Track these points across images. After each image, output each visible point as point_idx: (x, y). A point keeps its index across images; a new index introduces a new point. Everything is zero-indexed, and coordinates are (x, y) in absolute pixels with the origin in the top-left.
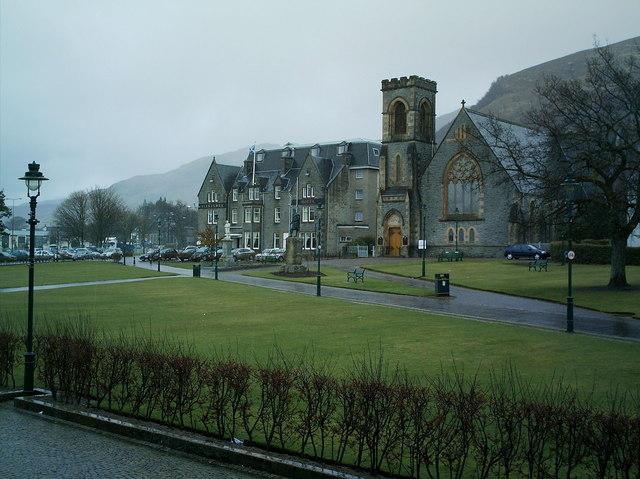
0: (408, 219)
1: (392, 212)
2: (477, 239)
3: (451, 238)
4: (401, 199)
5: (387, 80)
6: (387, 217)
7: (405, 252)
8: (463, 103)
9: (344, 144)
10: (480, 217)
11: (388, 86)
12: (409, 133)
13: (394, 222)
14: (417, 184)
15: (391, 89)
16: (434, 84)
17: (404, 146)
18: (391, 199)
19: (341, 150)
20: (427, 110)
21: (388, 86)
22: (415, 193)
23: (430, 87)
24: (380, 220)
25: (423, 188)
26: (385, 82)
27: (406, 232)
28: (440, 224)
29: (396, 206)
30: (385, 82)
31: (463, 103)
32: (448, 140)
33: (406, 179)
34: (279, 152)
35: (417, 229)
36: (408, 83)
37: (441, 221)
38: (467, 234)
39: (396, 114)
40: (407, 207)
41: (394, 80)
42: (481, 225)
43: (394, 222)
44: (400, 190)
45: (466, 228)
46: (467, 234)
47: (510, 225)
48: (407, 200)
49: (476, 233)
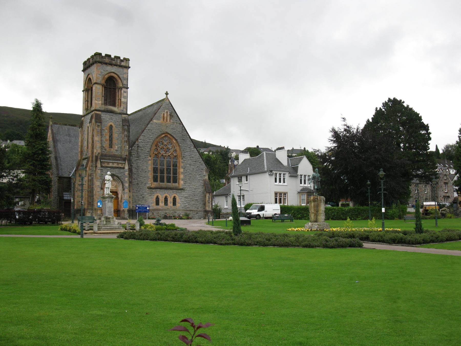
0: (127, 185)
2: (178, 205)
3: (157, 203)
4: (120, 166)
5: (100, 54)
7: (126, 215)
8: (167, 94)
10: (181, 187)
14: (130, 154)
15: (106, 64)
18: (111, 165)
25: (133, 159)
27: (126, 197)
31: (167, 94)
36: (123, 64)
37: (151, 188)
38: (170, 200)
40: (127, 173)
41: (108, 56)
46: (170, 200)
47: (207, 195)
48: (127, 167)
49: (178, 200)
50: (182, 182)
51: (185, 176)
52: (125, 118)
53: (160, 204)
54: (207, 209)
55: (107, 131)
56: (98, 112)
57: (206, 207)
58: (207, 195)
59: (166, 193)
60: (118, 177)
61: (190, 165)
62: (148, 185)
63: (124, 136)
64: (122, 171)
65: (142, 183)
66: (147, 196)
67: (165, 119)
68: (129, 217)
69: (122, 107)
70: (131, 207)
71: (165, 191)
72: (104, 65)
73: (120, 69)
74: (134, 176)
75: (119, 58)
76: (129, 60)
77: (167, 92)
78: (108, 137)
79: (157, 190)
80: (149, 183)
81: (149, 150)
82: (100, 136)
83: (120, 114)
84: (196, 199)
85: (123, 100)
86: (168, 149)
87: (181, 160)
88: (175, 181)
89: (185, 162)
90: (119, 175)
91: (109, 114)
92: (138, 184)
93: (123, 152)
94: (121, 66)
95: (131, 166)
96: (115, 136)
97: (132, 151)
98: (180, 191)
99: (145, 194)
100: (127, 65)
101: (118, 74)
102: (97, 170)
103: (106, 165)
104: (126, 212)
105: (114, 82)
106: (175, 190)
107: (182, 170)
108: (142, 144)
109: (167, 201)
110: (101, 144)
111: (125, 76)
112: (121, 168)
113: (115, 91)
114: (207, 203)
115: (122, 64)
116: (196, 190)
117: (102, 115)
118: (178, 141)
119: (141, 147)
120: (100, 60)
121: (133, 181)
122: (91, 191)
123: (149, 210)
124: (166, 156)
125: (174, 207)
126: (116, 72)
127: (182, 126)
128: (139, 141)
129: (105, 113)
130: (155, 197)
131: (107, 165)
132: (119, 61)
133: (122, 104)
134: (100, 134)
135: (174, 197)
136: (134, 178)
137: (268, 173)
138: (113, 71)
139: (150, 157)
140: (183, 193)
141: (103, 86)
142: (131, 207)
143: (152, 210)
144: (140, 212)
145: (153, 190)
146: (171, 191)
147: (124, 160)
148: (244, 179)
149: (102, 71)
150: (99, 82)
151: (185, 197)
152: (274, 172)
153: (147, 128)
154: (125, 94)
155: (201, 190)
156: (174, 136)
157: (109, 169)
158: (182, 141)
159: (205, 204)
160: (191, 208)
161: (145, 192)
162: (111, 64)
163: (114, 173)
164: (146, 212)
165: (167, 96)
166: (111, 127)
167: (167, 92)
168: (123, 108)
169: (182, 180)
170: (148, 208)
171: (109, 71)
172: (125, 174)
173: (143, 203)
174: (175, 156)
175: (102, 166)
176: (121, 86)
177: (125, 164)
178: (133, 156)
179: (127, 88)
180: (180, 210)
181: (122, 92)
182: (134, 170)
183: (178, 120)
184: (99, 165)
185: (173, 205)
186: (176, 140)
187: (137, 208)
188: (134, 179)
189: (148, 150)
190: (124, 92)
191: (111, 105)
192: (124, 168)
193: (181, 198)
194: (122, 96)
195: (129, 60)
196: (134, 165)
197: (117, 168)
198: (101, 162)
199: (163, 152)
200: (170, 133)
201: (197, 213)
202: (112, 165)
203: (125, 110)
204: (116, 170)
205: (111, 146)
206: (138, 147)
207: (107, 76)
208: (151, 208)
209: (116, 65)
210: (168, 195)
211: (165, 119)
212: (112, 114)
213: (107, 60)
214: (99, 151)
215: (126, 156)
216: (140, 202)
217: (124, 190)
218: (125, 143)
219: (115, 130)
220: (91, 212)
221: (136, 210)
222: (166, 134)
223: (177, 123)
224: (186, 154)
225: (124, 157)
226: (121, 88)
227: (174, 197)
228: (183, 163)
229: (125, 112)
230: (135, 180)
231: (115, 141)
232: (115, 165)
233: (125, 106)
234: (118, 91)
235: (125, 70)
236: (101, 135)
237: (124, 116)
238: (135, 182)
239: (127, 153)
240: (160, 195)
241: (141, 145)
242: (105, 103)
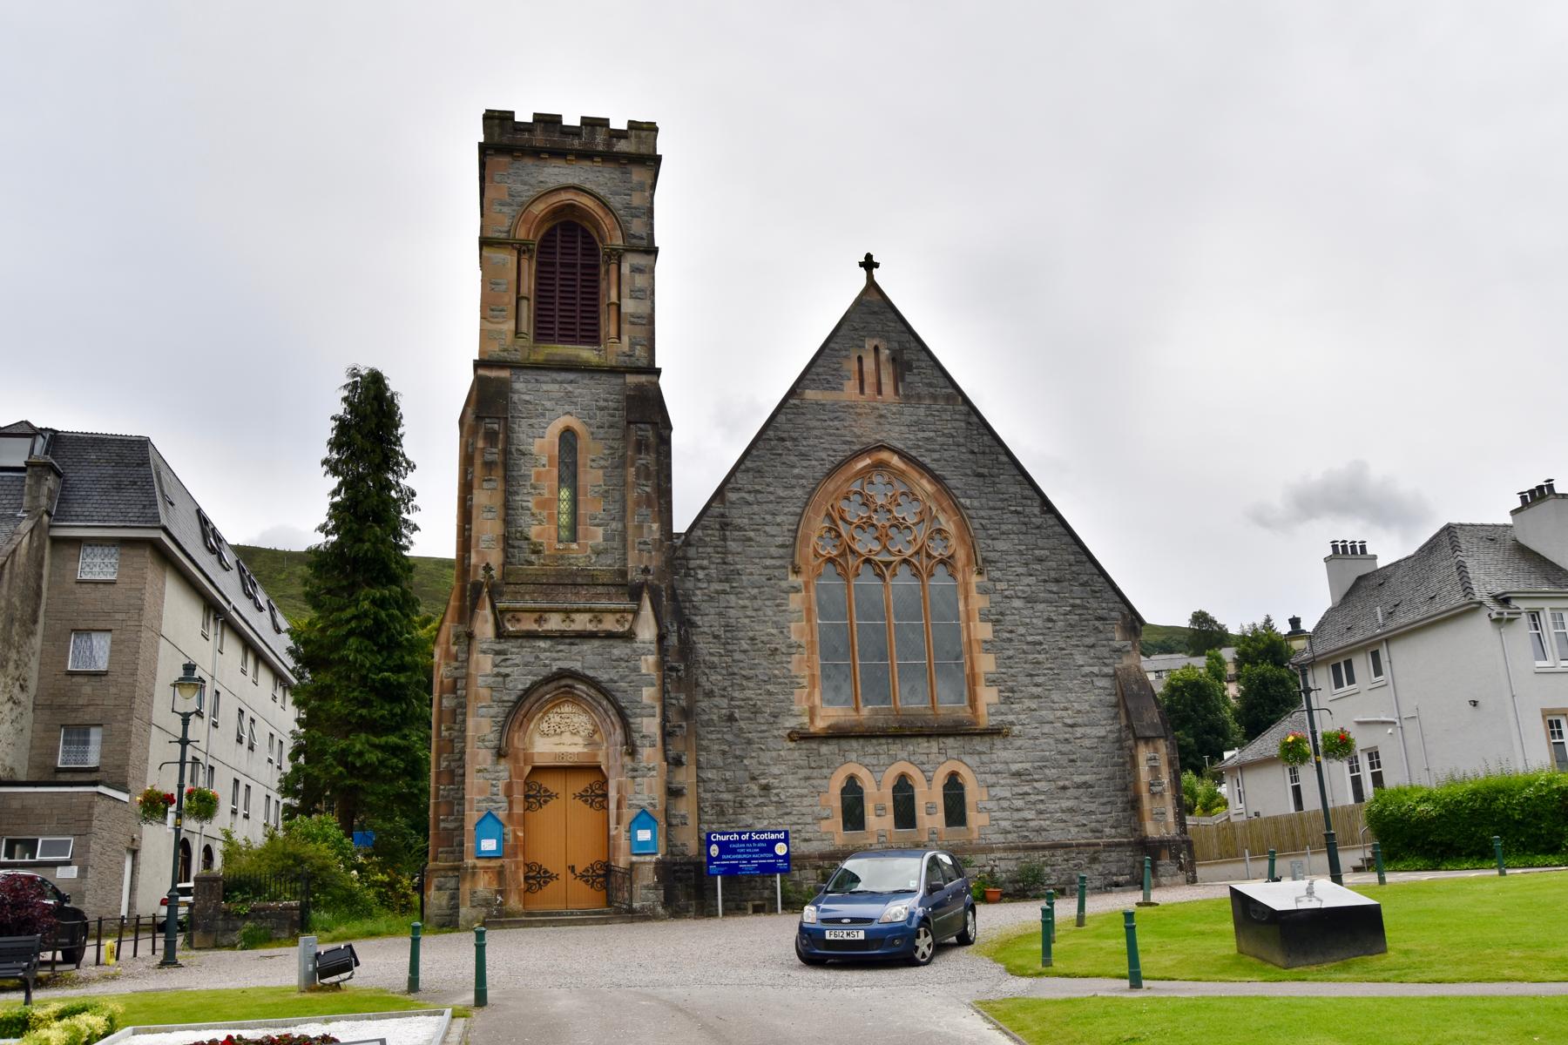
0: (650, 725)
2: (975, 819)
3: (853, 815)
4: (609, 624)
6: (520, 710)
7: (645, 891)
8: (869, 264)
10: (985, 721)
11: (505, 140)
13: (561, 736)
15: (535, 153)
18: (554, 623)
21: (505, 140)
25: (701, 588)
26: (497, 121)
27: (648, 791)
28: (796, 754)
30: (497, 121)
31: (869, 264)
32: (810, 394)
35: (686, 777)
36: (622, 146)
37: (800, 737)
38: (929, 796)
40: (648, 664)
41: (548, 122)
42: (1002, 753)
43: (561, 736)
46: (929, 796)
48: (647, 631)
50: (988, 696)
51: (1005, 662)
52: (639, 387)
53: (871, 819)
54: (1152, 830)
55: (544, 460)
56: (493, 374)
57: (1141, 820)
58: (1144, 753)
59: (903, 760)
60: (593, 683)
61: (1030, 600)
62: (791, 723)
63: (638, 476)
64: (620, 649)
65: (756, 711)
66: (791, 779)
67: (870, 379)
68: (668, 902)
69: (625, 339)
70: (692, 847)
71: (896, 748)
72: (528, 162)
75: (604, 122)
76: (652, 128)
77: (869, 257)
79: (845, 744)
80: (796, 708)
81: (789, 540)
82: (499, 485)
83: (614, 371)
84: (1078, 779)
85: (628, 306)
86: (898, 525)
87: (975, 579)
89: (1000, 586)
90: (603, 676)
91: (555, 375)
92: (731, 718)
93: (632, 555)
94: (610, 157)
95: (686, 624)
97: (692, 552)
98: (979, 744)
99: (775, 770)
100: (644, 150)
101: (601, 192)
102: (476, 656)
103: (528, 624)
104: (647, 876)
105: (587, 236)
106: (950, 741)
107: (984, 631)
108: (746, 510)
109: (912, 798)
110: (507, 521)
111: (637, 200)
112: (610, 635)
113: (597, 275)
114: (1145, 796)
115: (632, 152)
116: (1079, 731)
117: (518, 386)
118: (952, 483)
119: (741, 529)
120: (506, 140)
121: (704, 704)
122: (452, 773)
123: (786, 857)
124: (888, 564)
125: (955, 835)
126: (588, 186)
127: (964, 408)
128: (732, 496)
129: (530, 375)
130: (837, 782)
131: (535, 627)
132: (600, 138)
133: (625, 327)
134: (499, 472)
135: (953, 776)
136: (707, 686)
137: (1484, 613)
138: (571, 181)
139: (796, 571)
140: (1005, 755)
141: (522, 249)
142: (692, 847)
143: (822, 857)
144: (731, 872)
145: (824, 749)
146: (923, 745)
147: (635, 593)
148: (1362, 665)
149: (520, 187)
150: (503, 235)
151: (1018, 774)
152: (1523, 605)
153: (771, 433)
154: (640, 281)
155: (1101, 728)
156: (927, 460)
157: (542, 644)
158: (975, 480)
159: (1134, 804)
160: (1057, 836)
161: (778, 760)
162: (559, 153)
163: (577, 666)
164: (769, 870)
165: (870, 277)
166: (568, 438)
167: (869, 257)
168: (633, 345)
169: (992, 682)
170: (781, 849)
171: (551, 185)
172: (636, 669)
173: (761, 821)
174: (942, 562)
175: (501, 634)
176: (618, 241)
177: (636, 613)
178: (701, 574)
179: (653, 251)
180: (988, 849)
181: (625, 269)
182: (705, 647)
183: (942, 381)
184: (484, 627)
185: (949, 824)
186: (937, 479)
187: (714, 850)
188: (710, 694)
189: (779, 540)
190: (636, 270)
191: (568, 337)
192: (629, 636)
193: (991, 779)
194: (625, 290)
195: (656, 130)
196: (707, 621)
197: (592, 636)
198: (499, 616)
199: (866, 544)
200: (900, 446)
201: (1094, 860)
202: (563, 627)
203: (639, 351)
204: (587, 647)
206: (724, 526)
207: (539, 209)
208: (805, 848)
209: (586, 155)
210: (914, 772)
211: (870, 379)
212: (571, 376)
213: (539, 139)
214: (495, 558)
215: (646, 571)
216: (747, 819)
217: (632, 752)
218: (644, 510)
220: (452, 883)
221: (711, 859)
222: (885, 455)
223: (934, 397)
224: (1001, 545)
225: (634, 576)
226: (617, 255)
227: (953, 776)
228: (983, 591)
229: (643, 363)
230: (717, 700)
232: (582, 622)
233: (639, 332)
234: (607, 271)
235: (638, 175)
236: (507, 479)
237: (631, 379)
239: (655, 561)
240: (864, 775)
241: (739, 516)
242: (543, 333)
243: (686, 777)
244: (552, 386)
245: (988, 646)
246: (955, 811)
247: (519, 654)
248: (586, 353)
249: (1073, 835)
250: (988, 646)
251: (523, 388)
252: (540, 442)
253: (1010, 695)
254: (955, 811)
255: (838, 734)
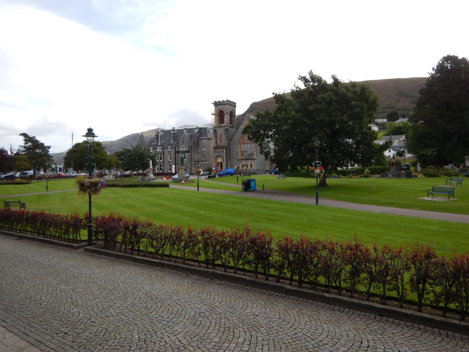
0: (225, 159)
1: (218, 156)
2: (253, 167)
9: (197, 128)
12: (225, 124)
14: (229, 144)
16: (235, 103)
17: (223, 129)
19: (196, 130)
20: (232, 114)
22: (228, 149)
23: (233, 105)
24: (214, 159)
29: (220, 154)
33: (224, 142)
34: (170, 131)
35: (229, 163)
39: (220, 115)
41: (219, 102)
43: (220, 160)
44: (220, 147)
45: (249, 163)
47: (266, 162)
48: (225, 151)
50: (255, 156)
73: (224, 106)
74: (232, 155)
78: (219, 138)
88: (252, 155)
94: (224, 104)
96: (223, 137)
107: (255, 149)
141: (217, 116)
182: (232, 152)
196: (232, 150)
205: (221, 142)
213: (218, 104)
219: (223, 135)
231: (223, 140)
238: (232, 157)
242: (220, 123)
243: (229, 163)
244: (220, 129)
245: (255, 151)
246: (251, 167)
247: (216, 153)
248: (222, 125)
249: (261, 169)
250: (255, 151)
251: (218, 129)
252: (219, 134)
253: (257, 156)
254: (251, 167)
255: (242, 159)
